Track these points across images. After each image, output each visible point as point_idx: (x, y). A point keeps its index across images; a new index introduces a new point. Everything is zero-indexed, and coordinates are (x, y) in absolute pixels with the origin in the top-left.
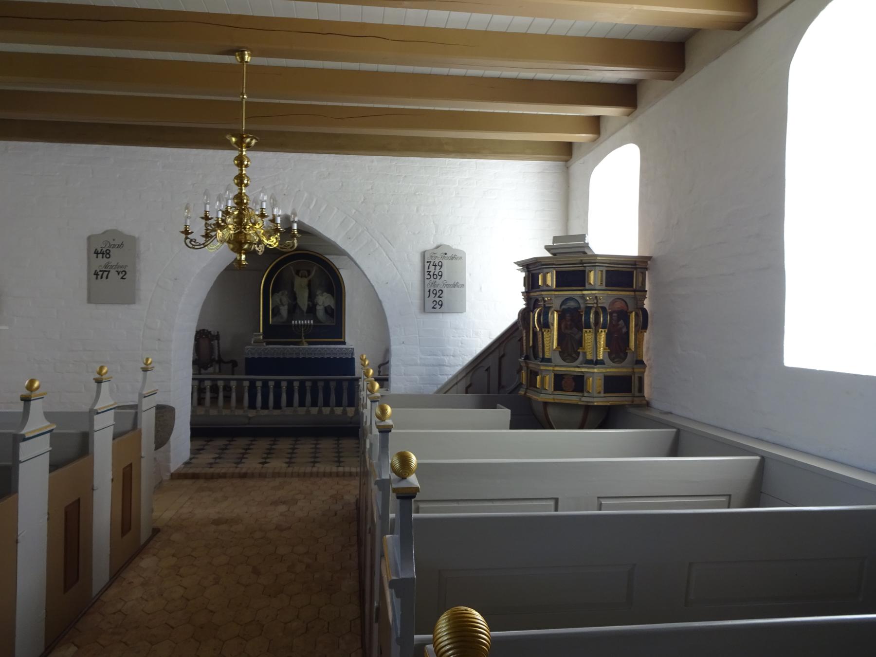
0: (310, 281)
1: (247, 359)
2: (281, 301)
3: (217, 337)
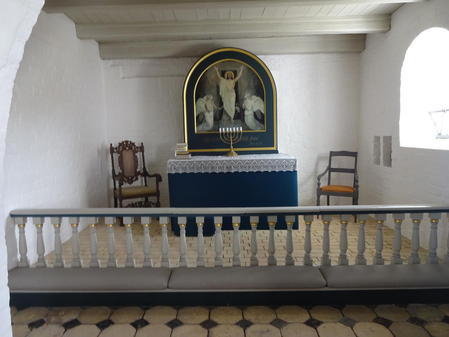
0: (237, 84)
1: (170, 175)
2: (206, 107)
3: (142, 149)
